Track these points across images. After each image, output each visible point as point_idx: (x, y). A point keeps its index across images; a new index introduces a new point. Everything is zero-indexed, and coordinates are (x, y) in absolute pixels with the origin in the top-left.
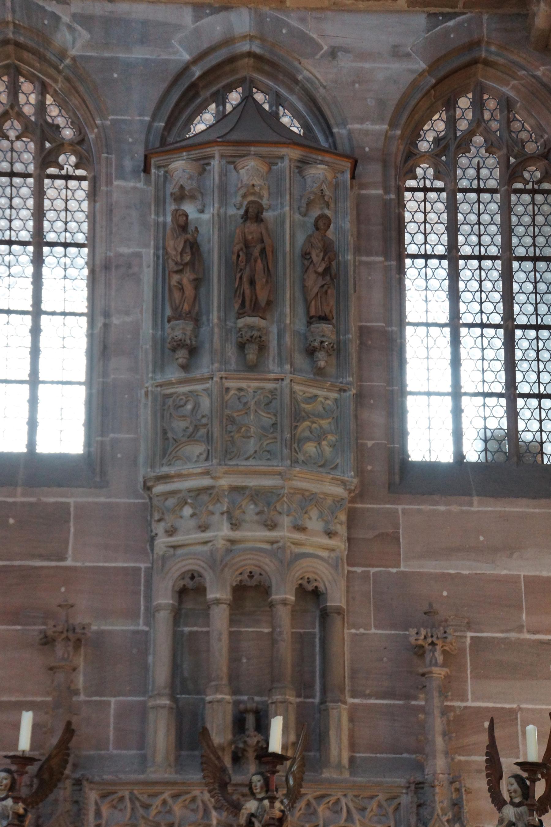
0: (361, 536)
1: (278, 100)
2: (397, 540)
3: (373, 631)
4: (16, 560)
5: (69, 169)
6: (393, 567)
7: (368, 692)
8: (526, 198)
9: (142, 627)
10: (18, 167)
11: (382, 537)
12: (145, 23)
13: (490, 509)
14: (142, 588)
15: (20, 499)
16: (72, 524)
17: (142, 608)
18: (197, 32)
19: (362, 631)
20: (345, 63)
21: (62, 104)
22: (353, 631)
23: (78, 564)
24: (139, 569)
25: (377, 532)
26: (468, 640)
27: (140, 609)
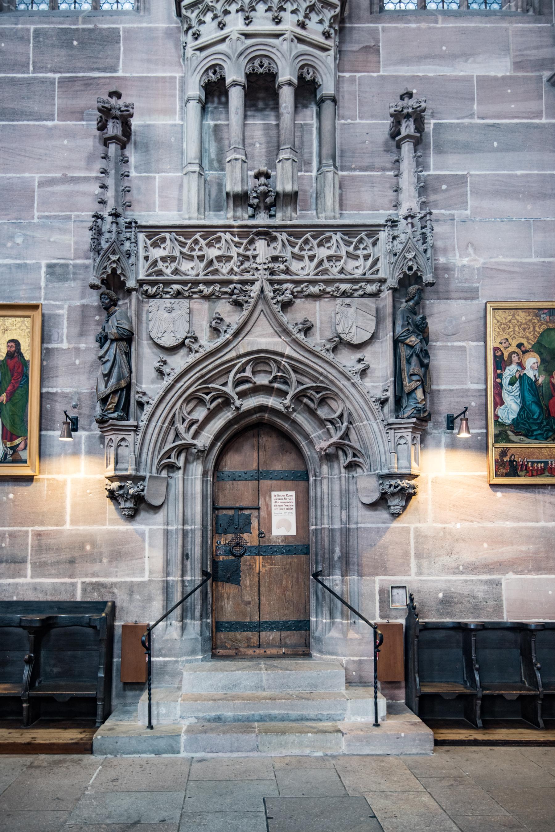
0: (349, 49)
3: (358, 121)
4: (80, 72)
6: (374, 72)
7: (353, 166)
9: (178, 122)
11: (366, 49)
13: (451, 25)
14: (177, 92)
15: (81, 26)
16: (121, 44)
17: (178, 107)
19: (349, 121)
22: (343, 121)
23: (127, 75)
24: (175, 78)
25: (362, 45)
26: (432, 126)
27: (175, 109)
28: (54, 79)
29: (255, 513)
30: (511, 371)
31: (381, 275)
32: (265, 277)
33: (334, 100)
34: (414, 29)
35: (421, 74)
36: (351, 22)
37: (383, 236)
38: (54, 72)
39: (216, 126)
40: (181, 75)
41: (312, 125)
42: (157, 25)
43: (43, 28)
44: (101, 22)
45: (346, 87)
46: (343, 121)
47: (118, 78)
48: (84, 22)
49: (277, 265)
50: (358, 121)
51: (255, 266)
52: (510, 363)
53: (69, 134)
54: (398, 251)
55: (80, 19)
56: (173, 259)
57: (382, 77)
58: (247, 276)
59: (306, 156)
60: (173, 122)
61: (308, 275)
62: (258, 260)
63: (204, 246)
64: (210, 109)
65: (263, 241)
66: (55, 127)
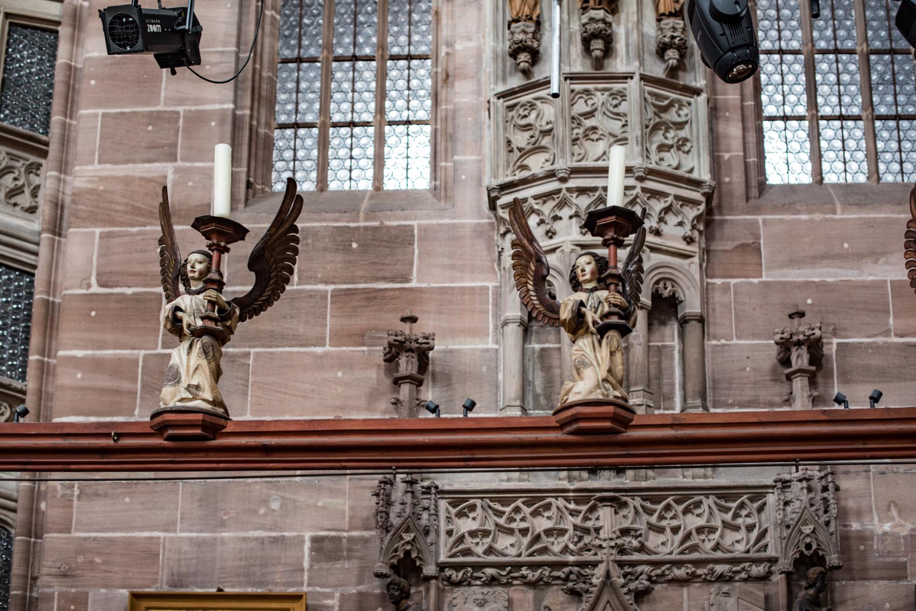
0: (720, 248)
2: (758, 250)
3: (735, 341)
4: (360, 283)
6: (754, 277)
7: (730, 401)
9: (491, 345)
13: (854, 216)
14: (491, 307)
15: (362, 224)
16: (416, 246)
17: (491, 326)
19: (723, 341)
22: (714, 342)
23: (423, 285)
24: (487, 288)
25: (736, 243)
26: (835, 347)
27: (488, 328)
28: (326, 292)
31: (771, 552)
32: (612, 558)
33: (701, 320)
34: (806, 221)
35: (817, 280)
36: (721, 214)
37: (771, 499)
38: (326, 282)
39: (543, 350)
40: (495, 284)
41: (673, 347)
42: (463, 221)
43: (313, 227)
44: (389, 218)
45: (717, 298)
46: (714, 342)
47: (411, 290)
48: (367, 219)
49: (627, 539)
50: (735, 341)
51: (597, 542)
53: (345, 363)
54: (791, 522)
55: (362, 215)
56: (486, 533)
57: (766, 284)
58: (588, 557)
59: (665, 389)
60: (485, 346)
61: (671, 553)
62: (603, 534)
63: (528, 516)
64: (535, 328)
65: (609, 508)
66: (326, 355)
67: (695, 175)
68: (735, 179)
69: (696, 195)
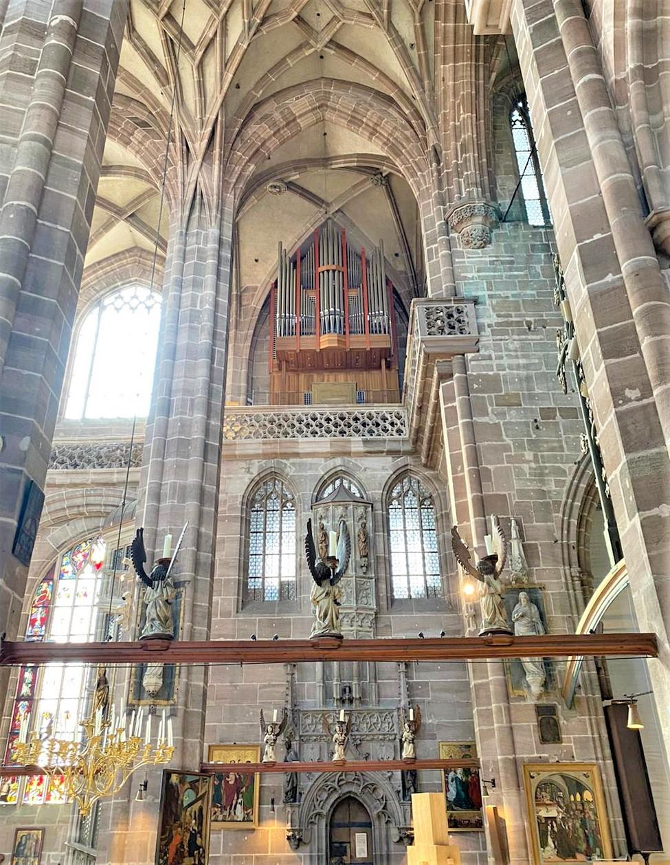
1: (350, 482)
5: (290, 508)
8: (426, 510)
10: (275, 508)
12: (311, 464)
18: (325, 466)
20: (369, 472)
21: (288, 488)
29: (348, 845)
30: (451, 775)
31: (395, 732)
52: (451, 771)
67: (371, 606)
68: (384, 603)
69: (372, 612)
